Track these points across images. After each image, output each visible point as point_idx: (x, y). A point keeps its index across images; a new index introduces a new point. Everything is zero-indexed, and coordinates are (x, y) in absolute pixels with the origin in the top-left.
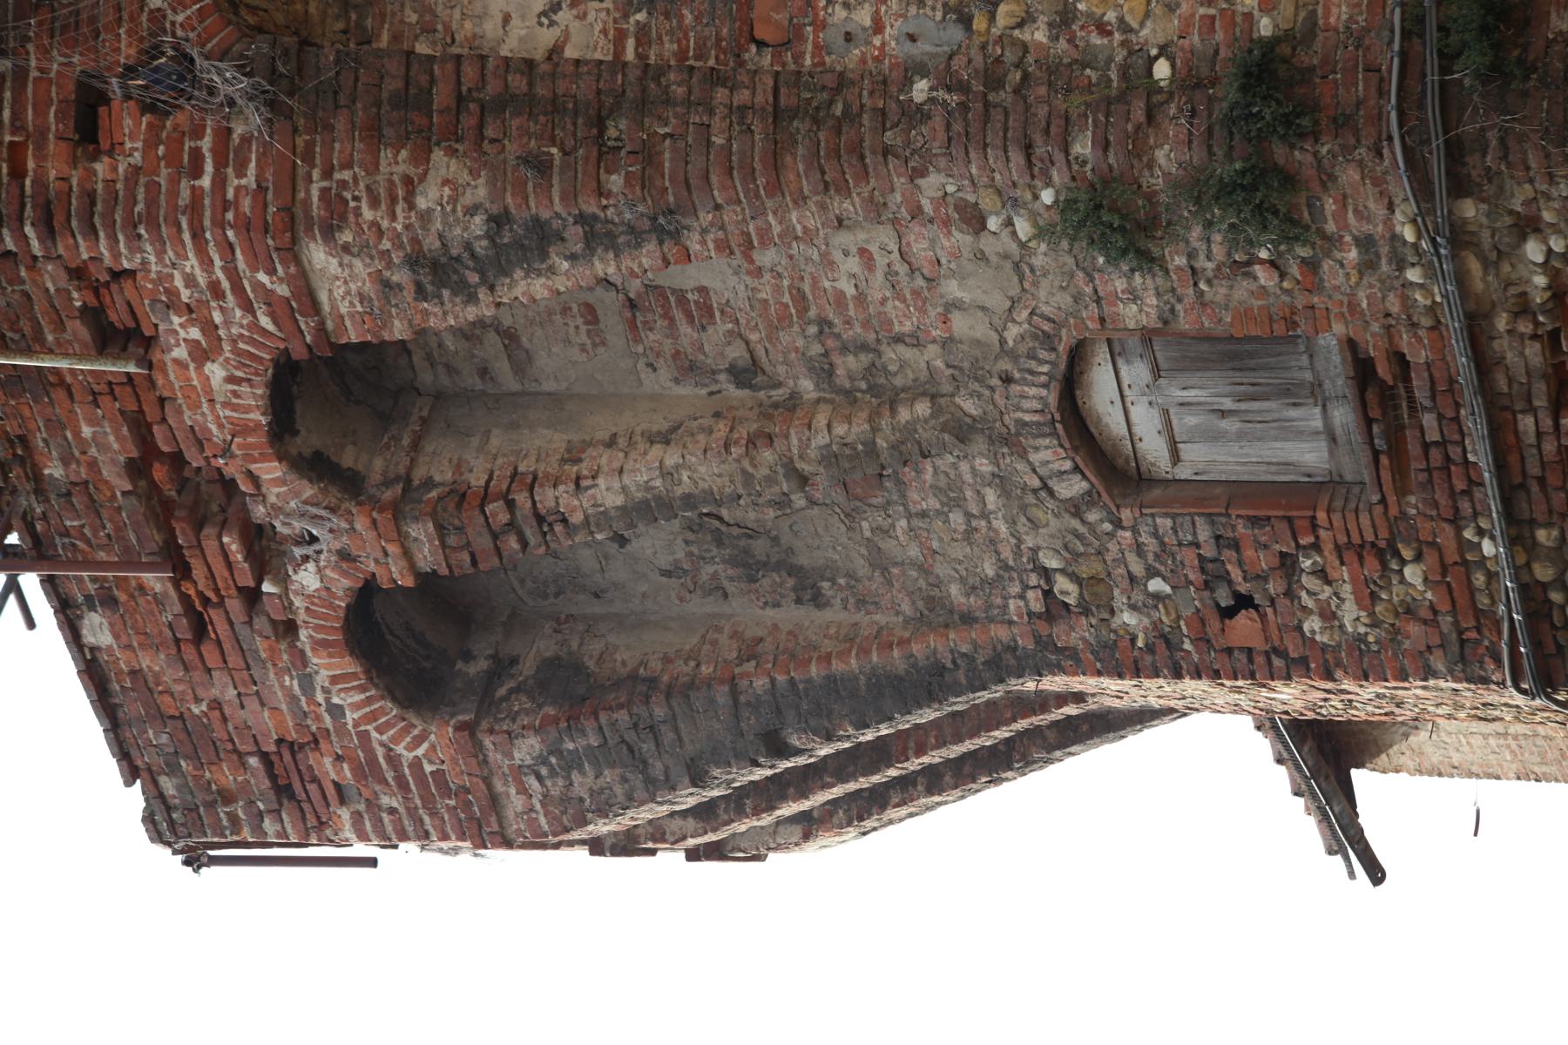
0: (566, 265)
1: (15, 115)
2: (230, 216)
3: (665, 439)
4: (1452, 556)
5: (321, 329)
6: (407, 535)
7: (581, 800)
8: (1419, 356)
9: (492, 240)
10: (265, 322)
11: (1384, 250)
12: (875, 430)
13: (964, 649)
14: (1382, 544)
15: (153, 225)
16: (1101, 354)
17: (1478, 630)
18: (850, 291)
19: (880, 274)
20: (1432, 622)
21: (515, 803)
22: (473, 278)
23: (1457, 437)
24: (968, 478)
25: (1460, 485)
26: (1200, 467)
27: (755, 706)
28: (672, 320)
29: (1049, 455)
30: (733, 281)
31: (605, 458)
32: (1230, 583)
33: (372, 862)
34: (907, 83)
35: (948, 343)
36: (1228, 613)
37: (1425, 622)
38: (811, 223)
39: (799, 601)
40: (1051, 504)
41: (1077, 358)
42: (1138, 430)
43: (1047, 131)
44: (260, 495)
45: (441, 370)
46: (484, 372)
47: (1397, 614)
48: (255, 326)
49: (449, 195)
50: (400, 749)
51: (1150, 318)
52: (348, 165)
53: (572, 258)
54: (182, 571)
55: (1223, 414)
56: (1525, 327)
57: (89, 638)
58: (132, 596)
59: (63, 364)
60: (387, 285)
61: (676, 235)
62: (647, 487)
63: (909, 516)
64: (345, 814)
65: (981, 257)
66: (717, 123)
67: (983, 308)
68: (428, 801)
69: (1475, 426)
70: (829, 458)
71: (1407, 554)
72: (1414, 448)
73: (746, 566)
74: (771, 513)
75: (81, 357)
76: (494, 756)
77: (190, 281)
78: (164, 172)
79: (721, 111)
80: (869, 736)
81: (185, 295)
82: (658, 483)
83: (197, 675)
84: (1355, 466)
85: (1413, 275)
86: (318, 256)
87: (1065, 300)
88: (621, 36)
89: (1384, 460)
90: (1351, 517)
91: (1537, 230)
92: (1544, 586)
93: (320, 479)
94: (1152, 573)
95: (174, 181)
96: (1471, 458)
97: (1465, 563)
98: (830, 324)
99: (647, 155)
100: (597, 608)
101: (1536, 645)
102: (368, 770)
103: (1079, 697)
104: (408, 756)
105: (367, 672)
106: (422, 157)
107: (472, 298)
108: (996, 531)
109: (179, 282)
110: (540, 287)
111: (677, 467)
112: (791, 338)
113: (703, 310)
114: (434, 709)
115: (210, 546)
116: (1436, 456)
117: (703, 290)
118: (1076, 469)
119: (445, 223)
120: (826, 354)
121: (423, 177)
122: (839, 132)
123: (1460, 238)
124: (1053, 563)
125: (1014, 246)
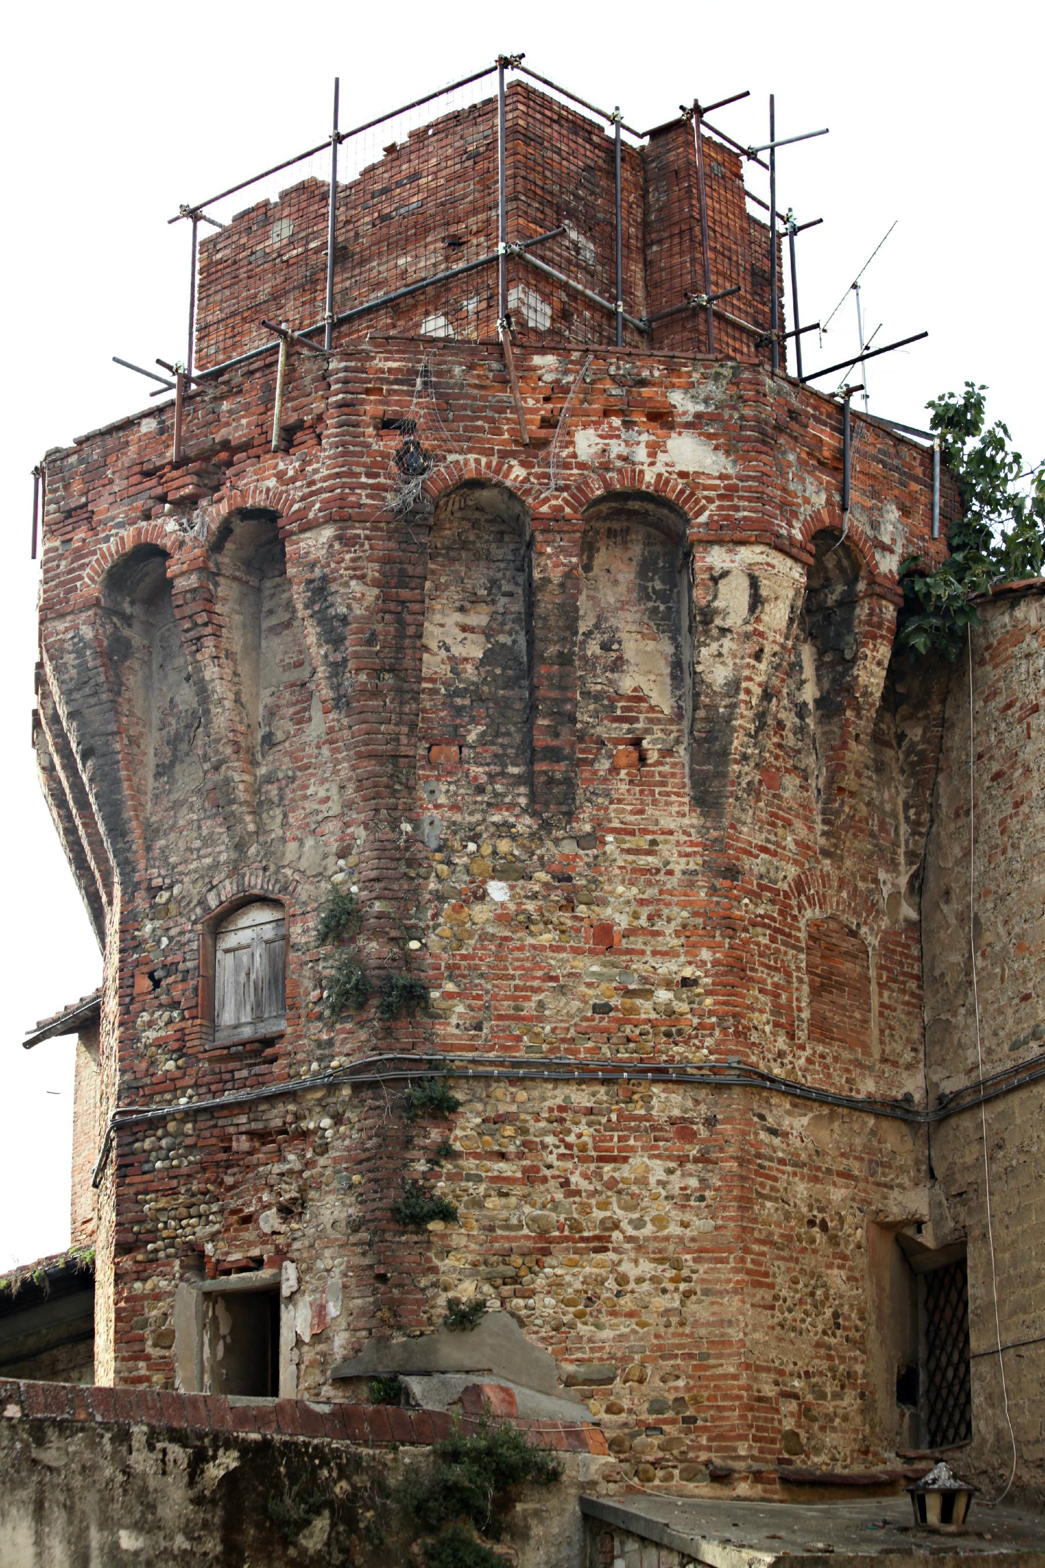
1: (396, 392)
3: (237, 700)
4: (179, 1083)
5: (292, 533)
8: (276, 1068)
10: (296, 507)
15: (343, 454)
16: (277, 915)
18: (309, 792)
21: (61, 626)
22: (316, 608)
25: (213, 1088)
27: (107, 744)
29: (228, 889)
30: (314, 734)
33: (34, 557)
34: (410, 821)
35: (283, 840)
36: (151, 976)
41: (276, 903)
44: (212, 503)
46: (271, 612)
48: (294, 502)
49: (356, 597)
52: (372, 548)
53: (326, 656)
54: (176, 466)
55: (248, 974)
56: (289, 1118)
57: (144, 421)
59: (276, 411)
60: (313, 565)
61: (337, 707)
62: (214, 691)
64: (57, 543)
65: (325, 856)
66: (392, 727)
68: (63, 584)
69: (243, 1095)
70: (227, 781)
71: (180, 1062)
72: (231, 1066)
76: (83, 616)
77: (316, 471)
79: (397, 729)
80: (92, 799)
81: (309, 469)
83: (125, 473)
84: (223, 1038)
85: (315, 1066)
86: (328, 533)
87: (304, 898)
88: (433, 681)
94: (171, 939)
95: (364, 465)
99: (376, 693)
100: (155, 666)
101: (137, 1123)
102: (78, 554)
103: (110, 903)
104: (84, 574)
106: (376, 583)
110: (312, 639)
112: (287, 763)
114: (107, 587)
115: (188, 479)
116: (228, 1076)
117: (310, 719)
123: (332, 1087)
124: (176, 890)
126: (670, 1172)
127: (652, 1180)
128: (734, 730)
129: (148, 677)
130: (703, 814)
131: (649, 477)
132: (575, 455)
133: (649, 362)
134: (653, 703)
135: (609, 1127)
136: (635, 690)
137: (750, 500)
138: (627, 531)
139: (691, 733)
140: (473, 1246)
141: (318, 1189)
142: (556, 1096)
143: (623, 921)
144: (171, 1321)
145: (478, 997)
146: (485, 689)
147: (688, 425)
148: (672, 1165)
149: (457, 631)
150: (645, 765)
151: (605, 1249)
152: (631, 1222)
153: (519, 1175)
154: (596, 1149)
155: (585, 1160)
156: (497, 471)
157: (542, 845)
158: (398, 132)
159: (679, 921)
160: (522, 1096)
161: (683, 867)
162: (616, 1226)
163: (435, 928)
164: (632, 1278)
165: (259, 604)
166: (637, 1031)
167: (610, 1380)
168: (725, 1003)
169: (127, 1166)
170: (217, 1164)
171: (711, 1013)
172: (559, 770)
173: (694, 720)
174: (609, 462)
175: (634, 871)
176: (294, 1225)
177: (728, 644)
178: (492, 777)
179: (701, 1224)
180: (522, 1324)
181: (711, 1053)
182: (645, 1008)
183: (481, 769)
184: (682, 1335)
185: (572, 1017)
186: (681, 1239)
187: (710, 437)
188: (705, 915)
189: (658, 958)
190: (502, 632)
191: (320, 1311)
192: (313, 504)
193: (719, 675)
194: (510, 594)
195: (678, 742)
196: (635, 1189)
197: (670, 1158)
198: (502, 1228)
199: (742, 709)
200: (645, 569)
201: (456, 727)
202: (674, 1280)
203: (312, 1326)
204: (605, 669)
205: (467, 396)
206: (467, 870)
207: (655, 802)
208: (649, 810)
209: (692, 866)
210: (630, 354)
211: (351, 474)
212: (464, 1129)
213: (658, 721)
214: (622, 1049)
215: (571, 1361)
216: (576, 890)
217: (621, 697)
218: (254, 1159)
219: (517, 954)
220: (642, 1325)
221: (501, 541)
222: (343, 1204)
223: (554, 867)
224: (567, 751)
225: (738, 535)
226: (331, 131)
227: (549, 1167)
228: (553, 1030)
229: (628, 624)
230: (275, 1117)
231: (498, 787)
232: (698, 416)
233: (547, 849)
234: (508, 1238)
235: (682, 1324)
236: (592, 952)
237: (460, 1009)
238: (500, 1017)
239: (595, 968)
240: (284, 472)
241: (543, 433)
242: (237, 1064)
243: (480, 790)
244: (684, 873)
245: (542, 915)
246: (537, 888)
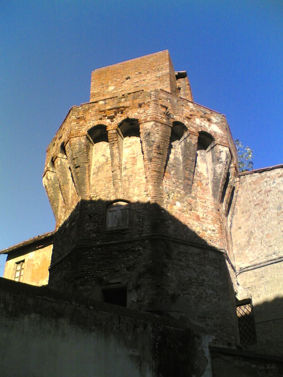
7: (75, 146)
8: (127, 236)
13: (87, 188)
28: (132, 161)
36: (89, 216)
39: (93, 172)
46: (125, 144)
49: (156, 137)
50: (84, 129)
52: (161, 128)
53: (147, 149)
62: (116, 155)
63: (105, 183)
77: (149, 112)
81: (146, 111)
82: (116, 156)
86: (152, 123)
107: (144, 138)
109: (148, 111)
111: (118, 158)
117: (136, 165)
132: (196, 122)
148: (214, 269)
151: (202, 286)
160: (185, 248)
168: (220, 236)
171: (218, 238)
175: (202, 206)
177: (221, 165)
181: (219, 246)
183: (174, 179)
192: (148, 117)
207: (205, 194)
219: (183, 218)
232: (216, 122)
237: (172, 227)
241: (190, 117)
246: (185, 205)
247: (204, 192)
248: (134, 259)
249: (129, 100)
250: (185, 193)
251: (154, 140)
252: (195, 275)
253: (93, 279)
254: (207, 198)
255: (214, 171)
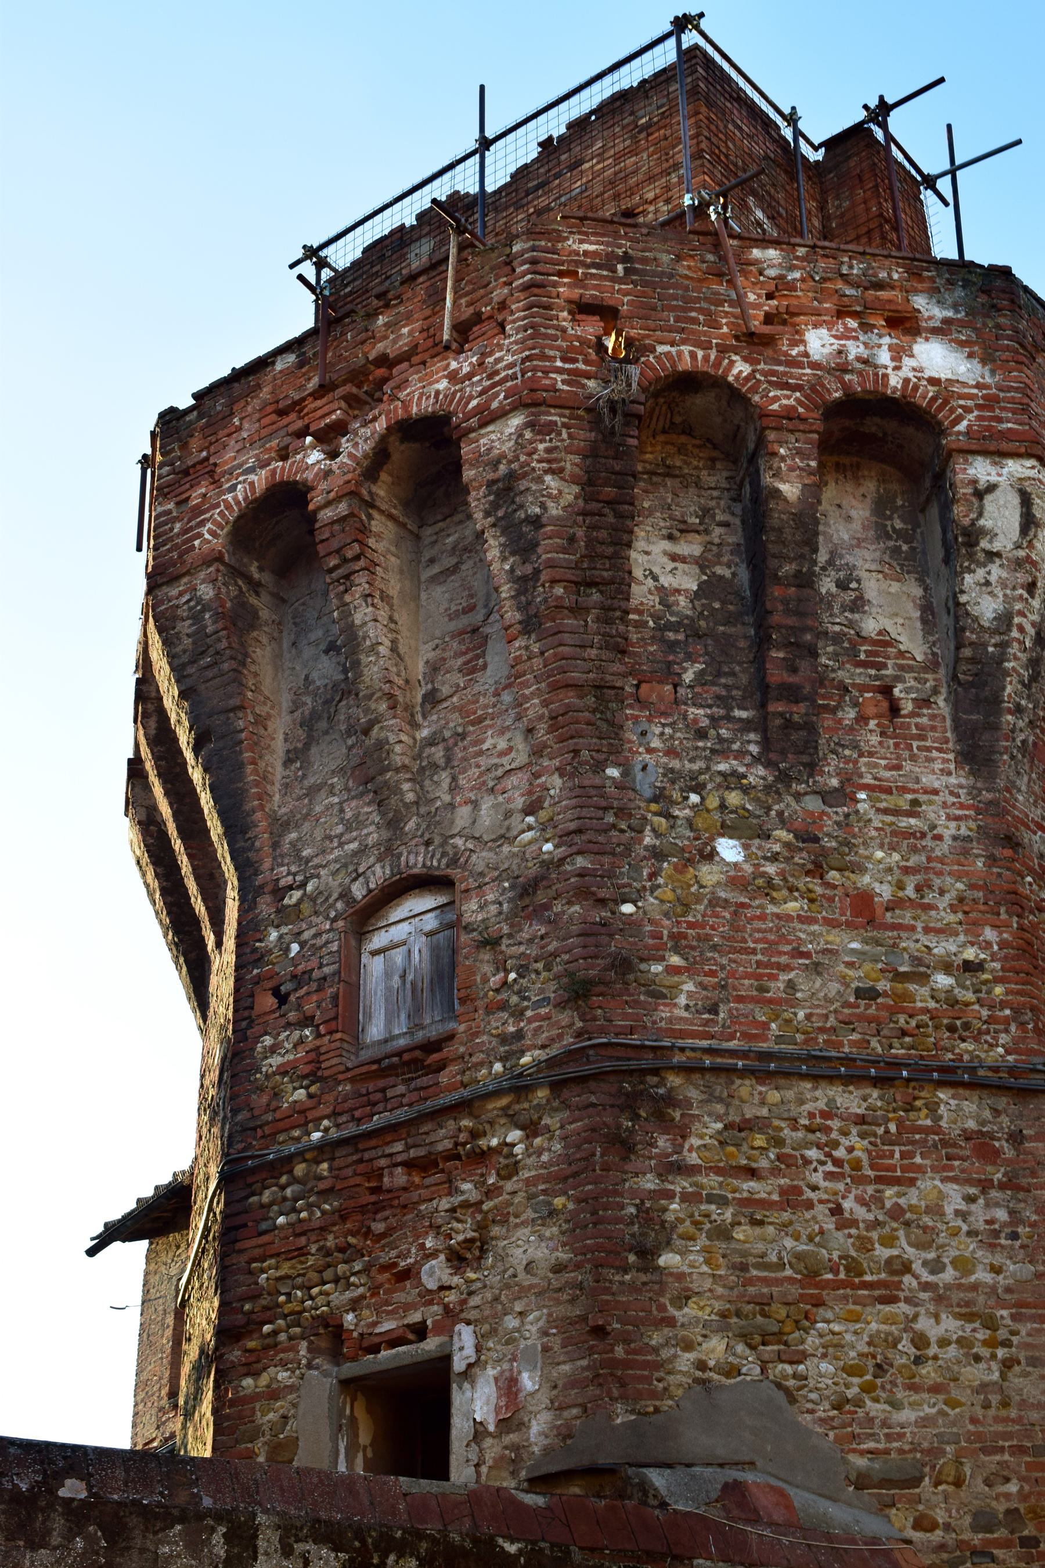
0: (507, 567)
2: (540, 374)
3: (394, 649)
4: (310, 1115)
5: (472, 430)
6: (340, 502)
8: (444, 1078)
9: (524, 521)
10: (474, 403)
11: (514, 1047)
12: (397, 770)
13: (257, 844)
14: (319, 1073)
15: (532, 337)
16: (442, 900)
17: (263, 1137)
18: (485, 747)
19: (496, 761)
20: (268, 1109)
22: (500, 513)
23: (389, 1107)
24: (365, 831)
26: (369, 968)
28: (465, 653)
29: (379, 874)
30: (491, 681)
31: (383, 614)
32: (296, 990)
33: (139, 549)
34: (617, 765)
35: (452, 806)
36: (276, 992)
37: (268, 1105)
38: (530, 712)
39: (288, 751)
40: (347, 880)
42: (393, 930)
43: (590, 842)
44: (365, 424)
45: (435, 537)
46: (432, 561)
47: (273, 1088)
48: (471, 398)
50: (209, 525)
51: (468, 918)
52: (570, 436)
53: (512, 570)
55: (403, 977)
56: (463, 1137)
58: (304, 374)
59: (448, 303)
60: (495, 464)
61: (526, 632)
63: (341, 803)
64: (171, 506)
65: (508, 815)
67: (474, 822)
72: (381, 1083)
73: (311, 719)
74: (343, 727)
75: (452, 313)
76: (202, 575)
78: (564, 344)
82: (368, 643)
85: (498, 1067)
86: (516, 421)
88: (640, 613)
89: (374, 1067)
90: (338, 1052)
91: (528, 1137)
92: (290, 1172)
93: (375, 454)
94: (302, 945)
95: (558, 348)
96: (375, 1118)
97: (306, 1124)
98: (463, 739)
99: (578, 610)
100: (286, 645)
102: (197, 511)
103: (219, 944)
104: (204, 531)
105: (256, 500)
106: (574, 480)
108: (331, 853)
109: (498, 355)
111: (378, 654)
112: (455, 721)
113: (471, 669)
114: (231, 543)
115: (336, 405)
116: (379, 1096)
117: (485, 667)
118: (370, 891)
119: (535, 491)
120: (444, 740)
121: (563, 479)
122: (589, 724)
124: (309, 888)
125: (515, 833)
126: (970, 1199)
127: (949, 1210)
128: (1006, 673)
129: (278, 656)
130: (972, 773)
131: (895, 381)
132: (806, 355)
133: (887, 263)
134: (902, 647)
135: (888, 1139)
136: (880, 633)
137: (1014, 412)
138: (858, 467)
139: (954, 677)
140: (720, 1290)
141: (505, 1222)
142: (818, 1097)
143: (885, 892)
144: (292, 1425)
145: (712, 973)
146: (702, 623)
147: (936, 331)
148: (972, 1191)
149: (665, 559)
150: (899, 716)
151: (892, 1300)
152: (925, 1263)
153: (775, 1197)
154: (872, 1167)
155: (860, 1180)
156: (718, 364)
157: (780, 800)
158: (555, 124)
159: (954, 894)
160: (774, 1096)
161: (953, 832)
162: (906, 1268)
163: (652, 891)
164: (933, 1340)
165: (418, 552)
166: (913, 1023)
167: (915, 1482)
168: (1019, 993)
169: (237, 1228)
170: (363, 1209)
171: (1003, 1004)
172: (799, 711)
173: (957, 660)
174: (847, 363)
175: (894, 833)
176: (472, 1275)
177: (996, 572)
178: (714, 720)
179: (1016, 1270)
180: (792, 1399)
181: (1008, 1052)
182: (921, 996)
183: (701, 712)
184: (1007, 1420)
185: (831, 1001)
186: (994, 1288)
187: (962, 344)
188: (984, 887)
189: (931, 936)
190: (720, 563)
191: (509, 1387)
192: (497, 394)
193: (987, 608)
194: (726, 525)
195: (935, 691)
196: (927, 1220)
197: (969, 1182)
198: (757, 1266)
199: (1014, 649)
200: (882, 507)
201: (669, 664)
202: (989, 1343)
203: (497, 1410)
204: (844, 608)
205: (676, 286)
206: (690, 824)
207: (913, 758)
208: (907, 766)
209: (963, 831)
210: (864, 253)
211: (543, 357)
212: (701, 1137)
213: (910, 669)
214: (896, 1042)
215: (862, 1453)
216: (825, 852)
217: (865, 640)
218: (414, 1196)
220: (953, 1404)
221: (713, 468)
222: (541, 1238)
223: (796, 825)
224: (807, 689)
225: (1005, 446)
226: (477, 135)
227: (814, 1188)
228: (808, 1017)
229: (865, 561)
230: (442, 1138)
231: (723, 731)
232: (946, 321)
233: (788, 804)
234: (765, 1281)
235: (1005, 1404)
236: (848, 924)
237: (689, 986)
238: (740, 999)
239: (854, 945)
240: (456, 372)
241: (767, 329)
242: (391, 1080)
243: (702, 734)
244: (955, 838)
245: (785, 880)
246: (777, 848)
247: (910, 747)
248: (481, 1202)
249: (408, 317)
250: (778, 779)
251: (538, 510)
252: (841, 1243)
253: (298, 1330)
254: (929, 780)
255: (957, 619)
